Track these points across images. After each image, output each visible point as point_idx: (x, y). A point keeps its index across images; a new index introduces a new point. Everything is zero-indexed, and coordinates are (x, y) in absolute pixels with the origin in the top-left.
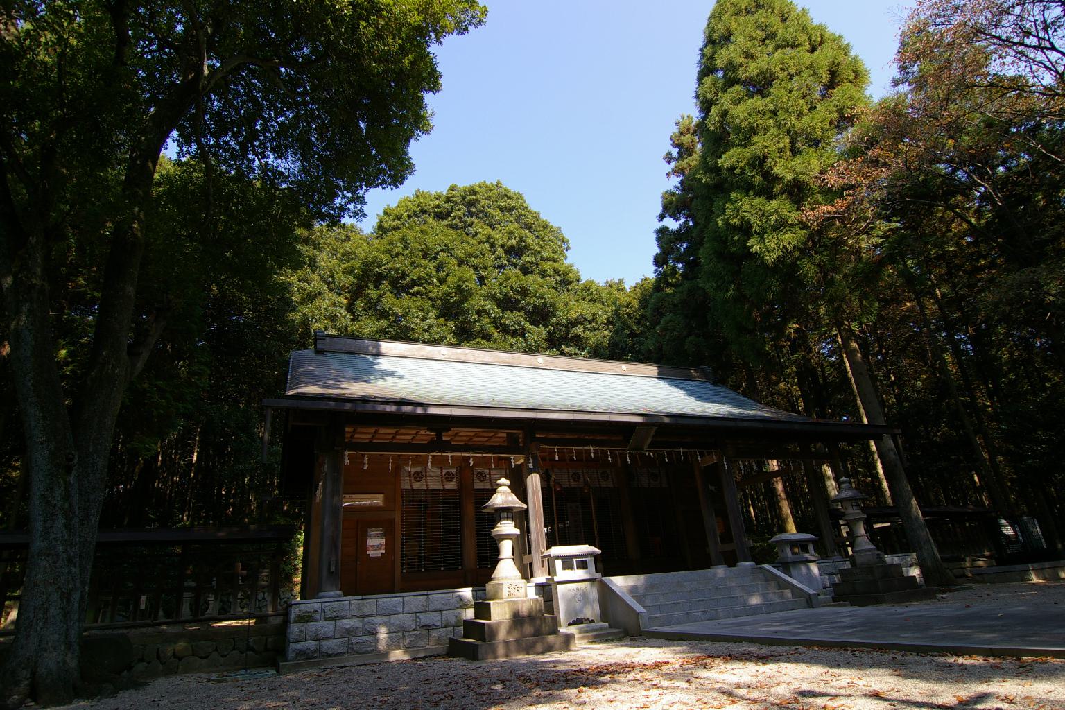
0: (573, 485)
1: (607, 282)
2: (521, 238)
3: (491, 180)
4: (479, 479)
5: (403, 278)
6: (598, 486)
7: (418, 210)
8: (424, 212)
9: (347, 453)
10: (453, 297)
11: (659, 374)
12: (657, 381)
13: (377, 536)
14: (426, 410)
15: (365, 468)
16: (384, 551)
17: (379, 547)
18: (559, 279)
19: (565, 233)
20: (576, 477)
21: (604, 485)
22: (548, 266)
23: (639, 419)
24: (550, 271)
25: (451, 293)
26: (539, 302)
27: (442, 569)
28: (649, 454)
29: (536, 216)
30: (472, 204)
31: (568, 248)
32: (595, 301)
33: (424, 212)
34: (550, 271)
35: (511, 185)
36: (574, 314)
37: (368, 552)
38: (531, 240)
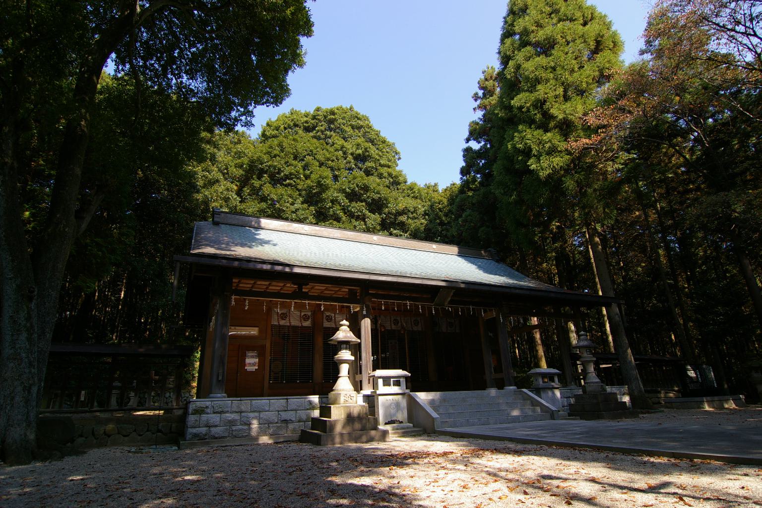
0: (394, 327)
1: (426, 184)
2: (366, 149)
3: (346, 105)
4: (327, 320)
5: (279, 173)
6: (411, 329)
7: (292, 124)
8: (296, 125)
9: (233, 297)
10: (314, 189)
11: (459, 253)
12: (456, 257)
13: (252, 357)
14: (292, 270)
15: (246, 308)
16: (257, 368)
17: (254, 365)
18: (392, 180)
19: (398, 148)
20: (396, 322)
21: (415, 328)
22: (384, 171)
23: (443, 284)
24: (386, 174)
25: (313, 186)
26: (376, 196)
27: (298, 381)
28: (448, 309)
29: (378, 134)
30: (331, 122)
31: (399, 159)
32: (416, 198)
33: (296, 125)
34: (386, 174)
35: (361, 109)
36: (401, 207)
37: (246, 368)
38: (373, 151)
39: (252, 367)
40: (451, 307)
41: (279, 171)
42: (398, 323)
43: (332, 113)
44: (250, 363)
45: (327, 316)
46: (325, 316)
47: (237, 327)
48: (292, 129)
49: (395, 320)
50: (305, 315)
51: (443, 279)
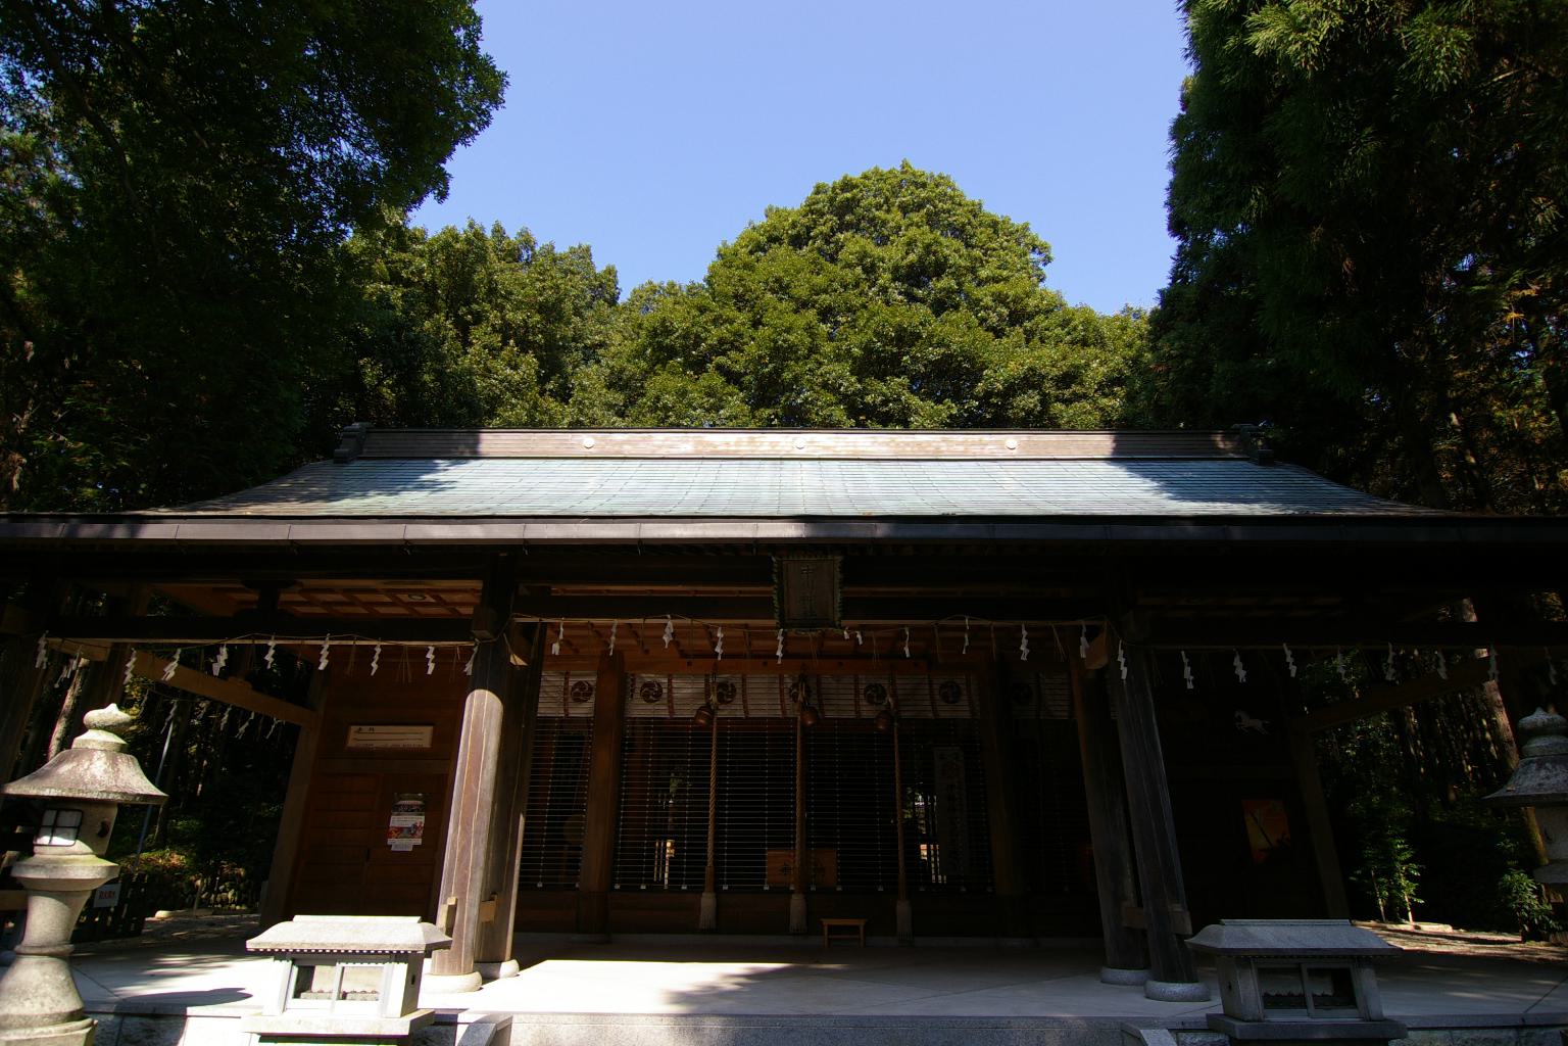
0: (867, 711)
1: (491, 58)
2: (927, 247)
3: (889, 164)
4: (646, 697)
5: (696, 345)
6: (930, 715)
7: (763, 239)
8: (773, 239)
9: (42, 642)
10: (767, 365)
11: (1116, 450)
12: (1103, 467)
13: (410, 810)
14: (134, 532)
15: (321, 667)
16: (419, 841)
17: (411, 832)
18: (1005, 311)
19: (1040, 232)
20: (876, 694)
21: (945, 711)
22: (985, 295)
23: (791, 531)
24: (988, 301)
25: (761, 357)
26: (934, 354)
27: (540, 885)
28: (853, 637)
29: (975, 211)
30: (850, 206)
31: (1047, 260)
32: (1085, 343)
33: (773, 239)
34: (988, 301)
35: (925, 165)
36: (1014, 368)
37: (390, 841)
38: (951, 249)
39: (405, 841)
40: (862, 628)
41: (698, 340)
42: (882, 696)
43: (847, 185)
44: (401, 829)
45: (646, 685)
46: (639, 685)
47: (378, 729)
48: (765, 251)
49: (870, 687)
50: (580, 683)
51: (801, 511)
